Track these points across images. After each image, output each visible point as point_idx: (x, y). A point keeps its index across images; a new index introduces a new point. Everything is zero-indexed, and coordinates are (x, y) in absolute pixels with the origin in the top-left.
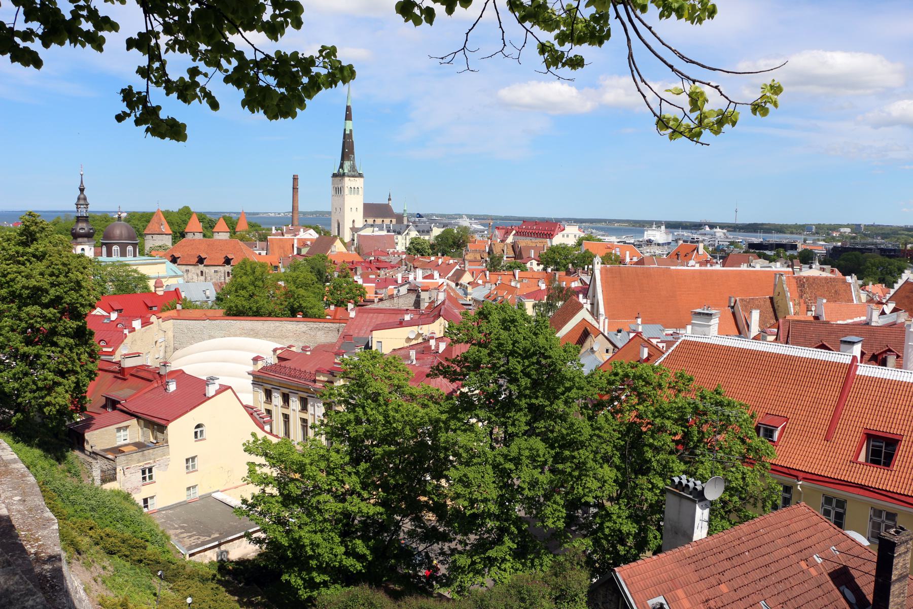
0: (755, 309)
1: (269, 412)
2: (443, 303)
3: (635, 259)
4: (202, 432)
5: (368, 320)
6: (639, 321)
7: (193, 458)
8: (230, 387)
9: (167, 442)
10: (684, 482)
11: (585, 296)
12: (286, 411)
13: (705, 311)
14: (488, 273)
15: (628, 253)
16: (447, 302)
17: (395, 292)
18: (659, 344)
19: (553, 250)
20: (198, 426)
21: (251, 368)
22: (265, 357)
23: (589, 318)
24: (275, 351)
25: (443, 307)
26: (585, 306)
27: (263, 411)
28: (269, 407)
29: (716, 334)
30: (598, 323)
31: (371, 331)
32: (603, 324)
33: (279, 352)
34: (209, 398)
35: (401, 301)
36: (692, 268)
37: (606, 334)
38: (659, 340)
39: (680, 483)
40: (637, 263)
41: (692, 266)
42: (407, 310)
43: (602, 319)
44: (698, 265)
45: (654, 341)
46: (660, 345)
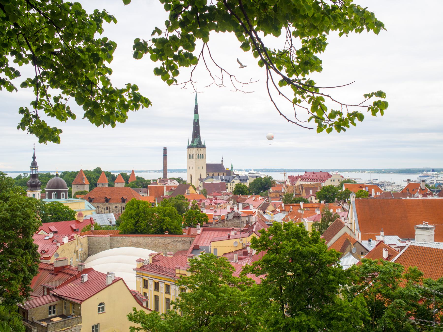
1: (145, 294)
2: (255, 224)
4: (103, 308)
5: (208, 235)
6: (382, 233)
7: (97, 326)
8: (122, 279)
9: (80, 315)
12: (156, 293)
13: (425, 226)
14: (283, 205)
15: (373, 190)
16: (257, 223)
17: (226, 218)
19: (324, 189)
20: (101, 304)
21: (135, 267)
22: (144, 260)
23: (348, 232)
24: (150, 255)
25: (255, 227)
26: (345, 224)
27: (142, 294)
28: (145, 290)
31: (210, 242)
32: (358, 236)
33: (153, 256)
34: (108, 286)
35: (230, 223)
36: (417, 198)
37: (360, 242)
40: (380, 196)
42: (233, 229)
43: (356, 232)
44: (422, 196)
45: (393, 247)
46: (397, 249)
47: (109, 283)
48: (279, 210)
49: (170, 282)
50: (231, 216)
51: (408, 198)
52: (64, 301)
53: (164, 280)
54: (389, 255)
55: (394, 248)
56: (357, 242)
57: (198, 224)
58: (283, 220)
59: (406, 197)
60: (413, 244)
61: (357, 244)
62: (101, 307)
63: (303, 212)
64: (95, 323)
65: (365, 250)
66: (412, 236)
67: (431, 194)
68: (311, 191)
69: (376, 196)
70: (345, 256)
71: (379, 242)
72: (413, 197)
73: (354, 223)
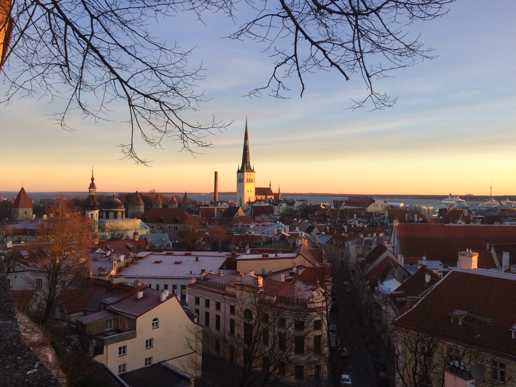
0: (506, 251)
1: (197, 311)
3: (421, 219)
4: (157, 323)
6: (424, 258)
10: (457, 365)
11: (389, 242)
12: (207, 310)
15: (416, 216)
18: (438, 273)
20: (155, 319)
23: (391, 255)
26: (388, 248)
28: (197, 307)
29: (476, 267)
30: (398, 258)
34: (162, 302)
36: (460, 225)
37: (403, 266)
38: (438, 271)
39: (454, 366)
40: (421, 222)
41: (460, 224)
43: (399, 256)
45: (435, 271)
46: (439, 274)
47: (163, 301)
48: (324, 233)
49: (221, 299)
50: (278, 238)
51: (451, 224)
52: (120, 316)
53: (215, 298)
54: (431, 280)
55: (436, 273)
56: (400, 265)
57: (247, 245)
58: (328, 242)
59: (449, 224)
60: (455, 270)
61: (399, 268)
62: (155, 323)
63: (347, 236)
64: (148, 338)
65: (408, 274)
66: (454, 262)
67: (474, 222)
68: (355, 215)
69: (418, 222)
70: (388, 279)
71: (421, 266)
72: (456, 224)
73: (397, 248)
